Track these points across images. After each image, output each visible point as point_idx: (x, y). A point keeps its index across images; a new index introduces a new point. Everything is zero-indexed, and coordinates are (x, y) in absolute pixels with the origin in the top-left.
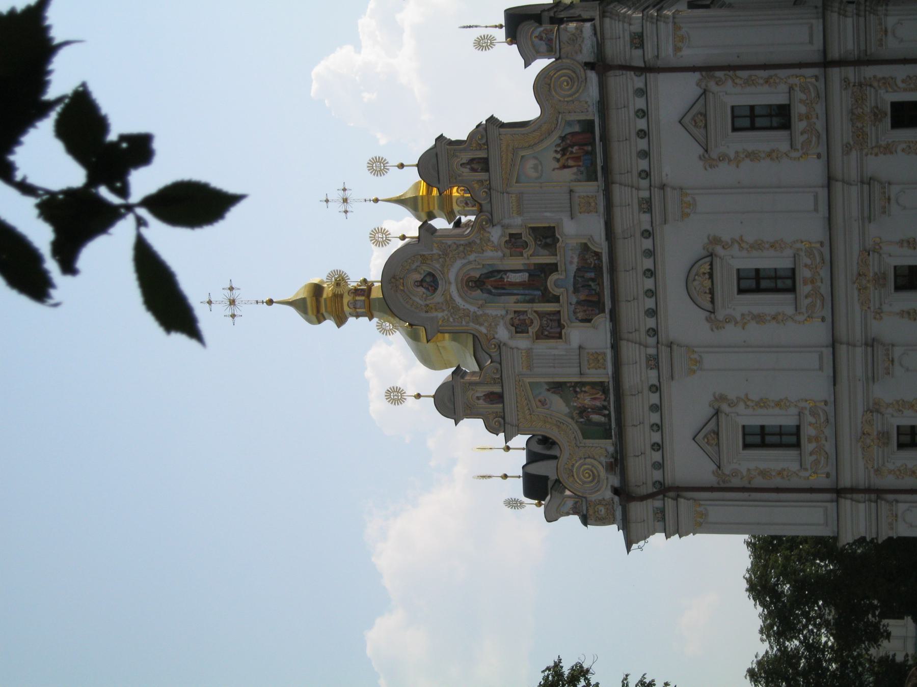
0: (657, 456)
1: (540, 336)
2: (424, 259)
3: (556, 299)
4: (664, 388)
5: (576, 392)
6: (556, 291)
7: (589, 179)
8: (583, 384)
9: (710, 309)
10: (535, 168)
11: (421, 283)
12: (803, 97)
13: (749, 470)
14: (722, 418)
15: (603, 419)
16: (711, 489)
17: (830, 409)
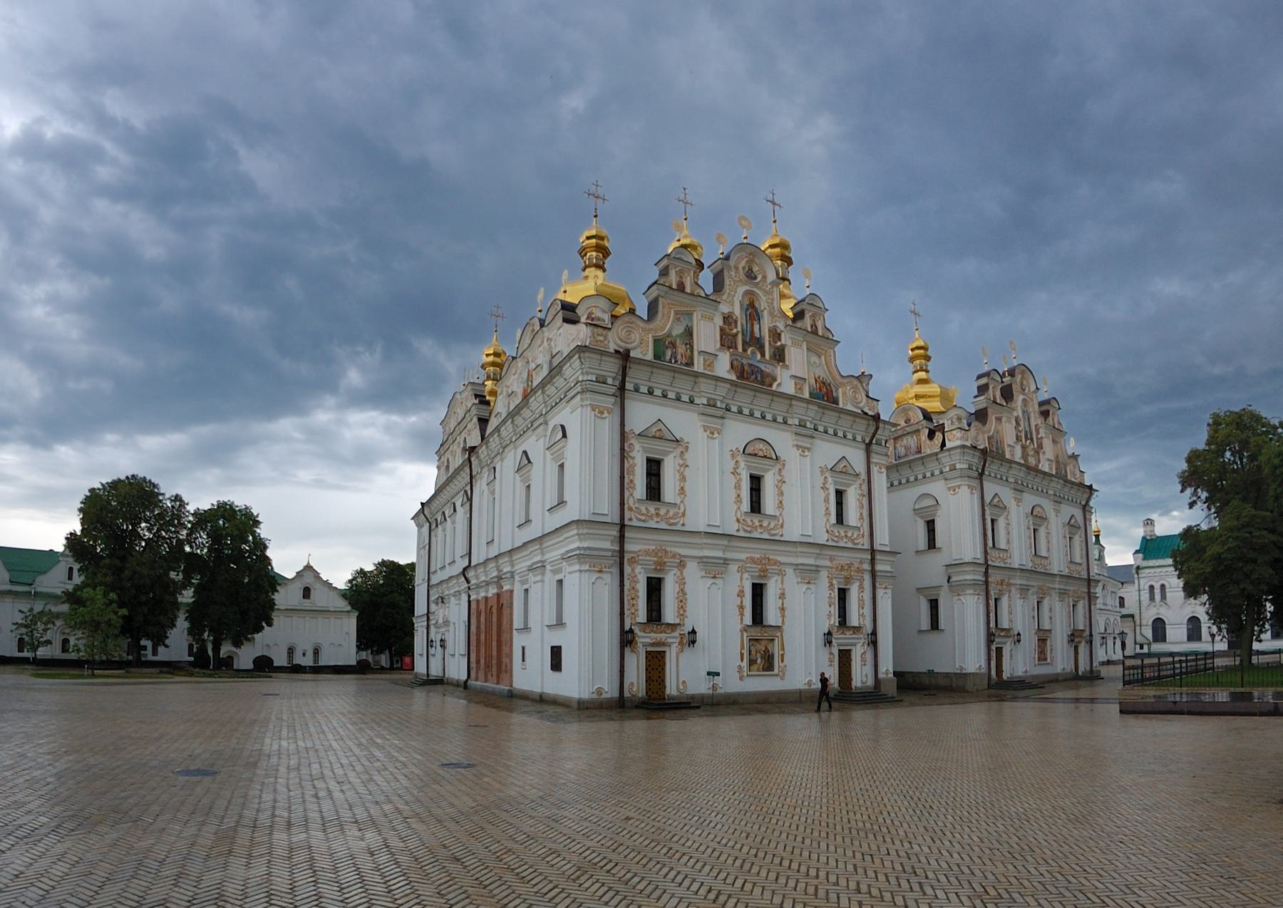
0: (644, 389)
1: (722, 329)
2: (764, 277)
3: (745, 350)
4: (691, 407)
5: (686, 344)
6: (749, 352)
7: (810, 393)
8: (692, 351)
9: (748, 450)
10: (815, 363)
11: (751, 269)
12: (855, 536)
13: (633, 458)
14: (674, 445)
15: (668, 358)
16: (622, 424)
17: (679, 527)
